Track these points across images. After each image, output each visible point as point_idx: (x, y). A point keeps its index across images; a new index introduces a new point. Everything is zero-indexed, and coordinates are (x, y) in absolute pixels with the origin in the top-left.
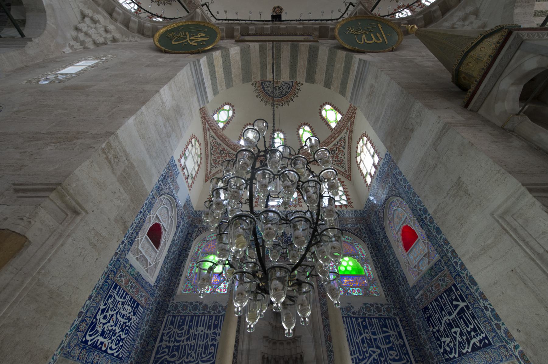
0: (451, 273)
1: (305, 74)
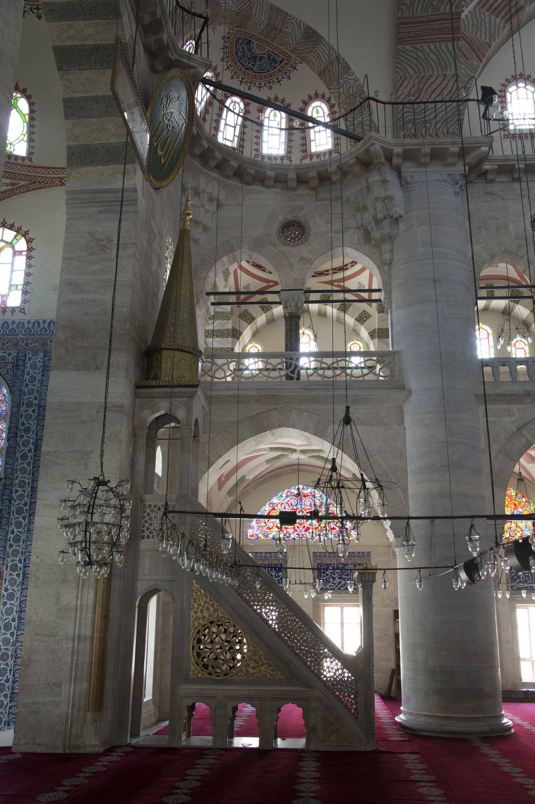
0: (3, 494)
1: (69, 43)
